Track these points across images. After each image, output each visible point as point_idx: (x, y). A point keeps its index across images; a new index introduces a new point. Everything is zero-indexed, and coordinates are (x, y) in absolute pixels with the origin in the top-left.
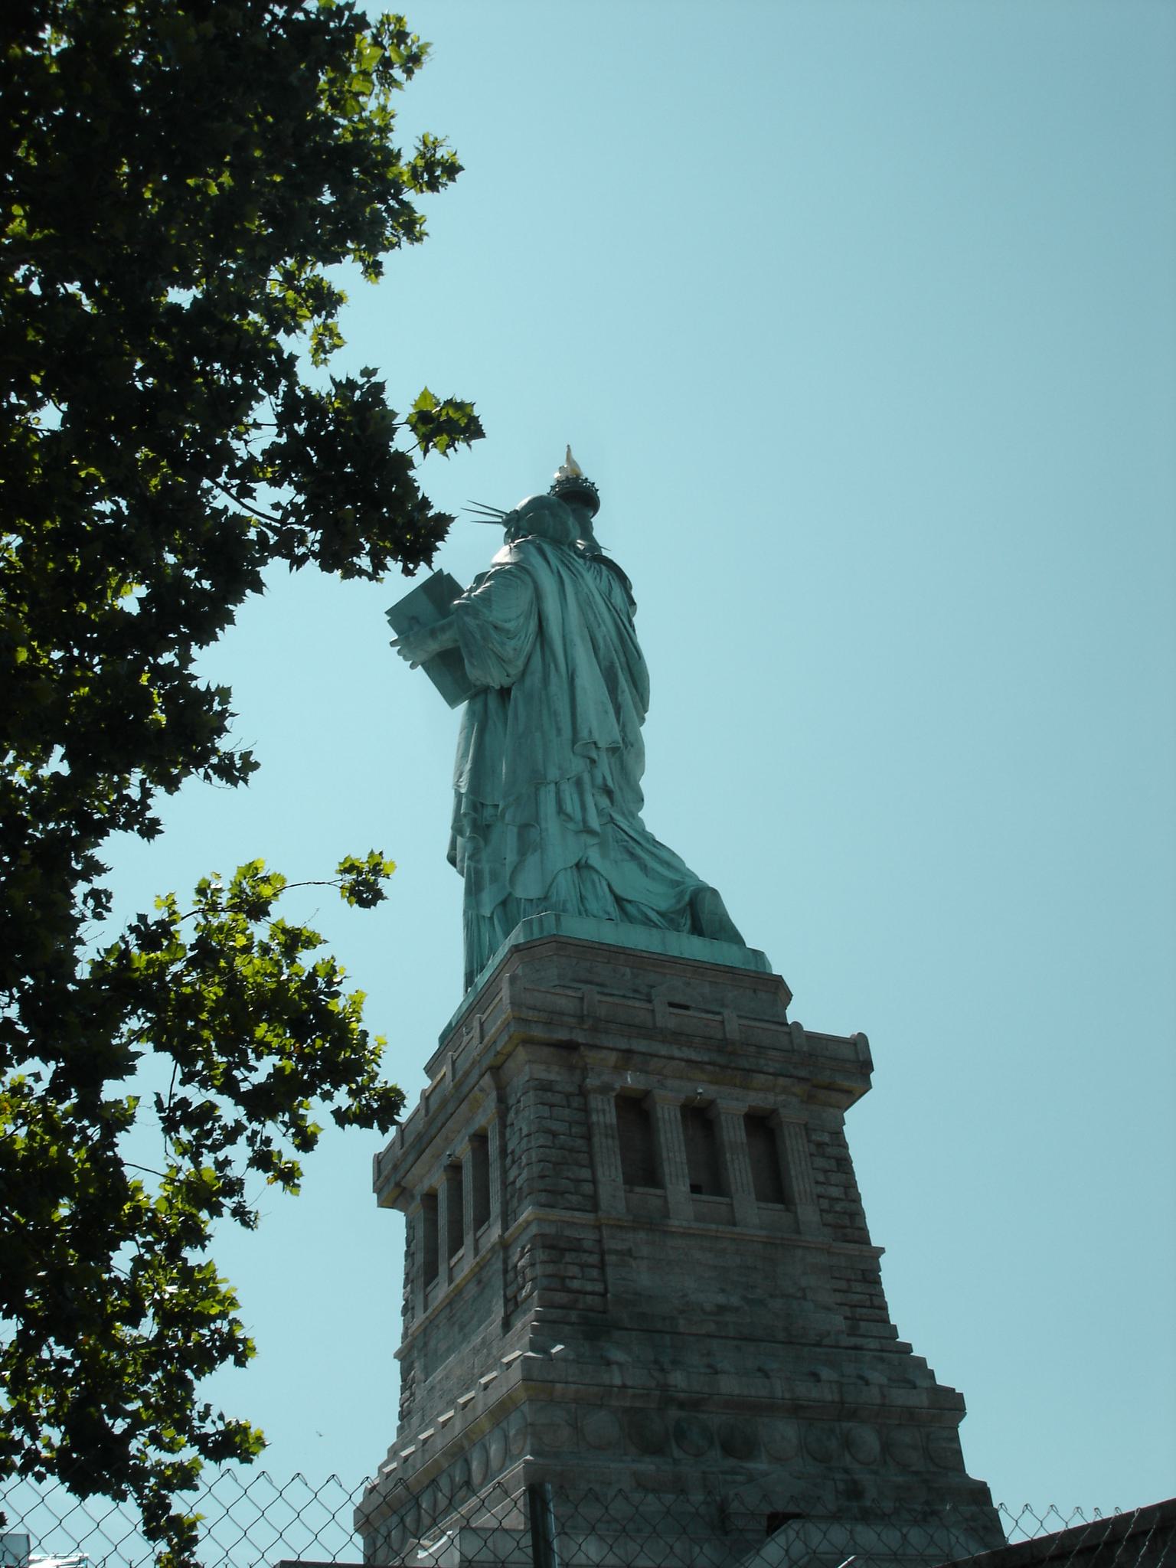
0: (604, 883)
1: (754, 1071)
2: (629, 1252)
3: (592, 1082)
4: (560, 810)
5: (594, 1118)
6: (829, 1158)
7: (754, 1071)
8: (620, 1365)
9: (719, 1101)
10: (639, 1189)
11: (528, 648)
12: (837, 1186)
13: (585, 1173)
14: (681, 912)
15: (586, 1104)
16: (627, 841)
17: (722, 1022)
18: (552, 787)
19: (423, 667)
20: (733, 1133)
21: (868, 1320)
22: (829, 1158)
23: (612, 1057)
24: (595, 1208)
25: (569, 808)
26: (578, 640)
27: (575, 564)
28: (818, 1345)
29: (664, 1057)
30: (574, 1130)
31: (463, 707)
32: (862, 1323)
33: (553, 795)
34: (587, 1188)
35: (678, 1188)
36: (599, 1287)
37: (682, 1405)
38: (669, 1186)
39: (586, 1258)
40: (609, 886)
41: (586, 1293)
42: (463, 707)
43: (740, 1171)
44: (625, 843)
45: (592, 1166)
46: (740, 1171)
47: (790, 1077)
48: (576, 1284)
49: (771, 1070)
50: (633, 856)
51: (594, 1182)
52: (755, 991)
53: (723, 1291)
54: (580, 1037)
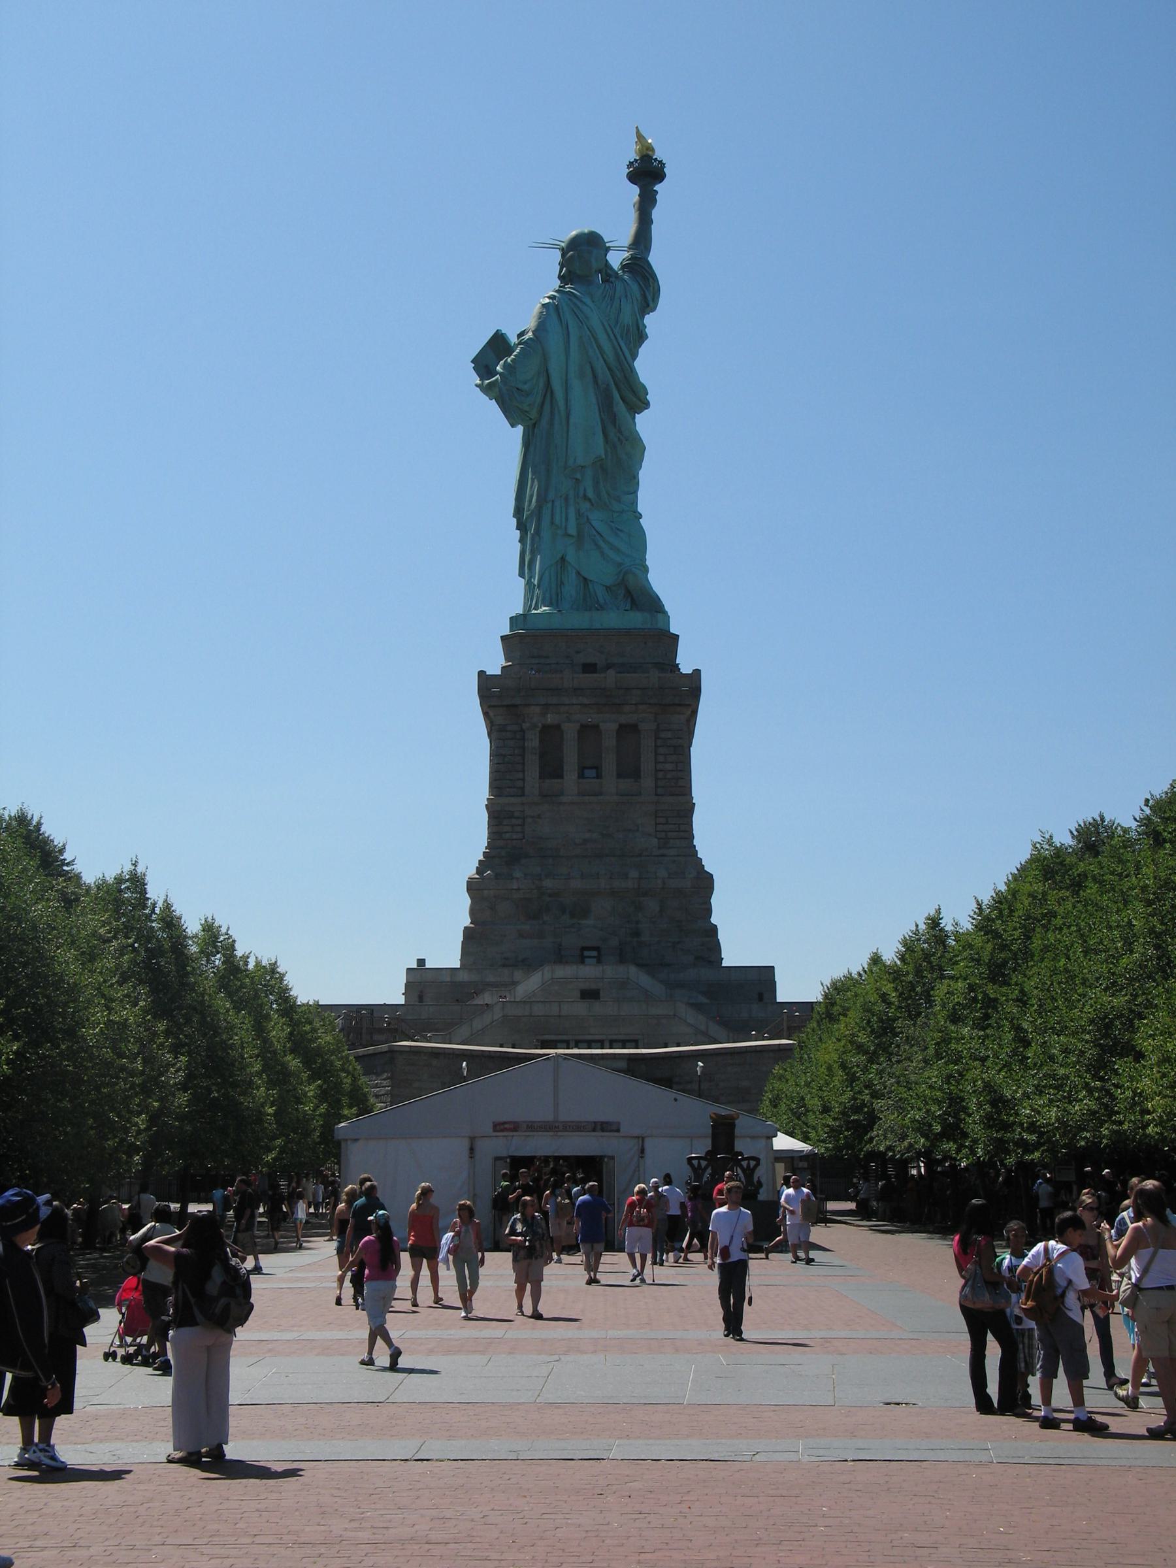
0: (574, 571)
1: (623, 704)
2: (539, 816)
3: (525, 726)
4: (552, 523)
5: (526, 745)
6: (670, 746)
7: (623, 704)
8: (517, 879)
9: (601, 724)
10: (548, 781)
11: (539, 400)
12: (671, 763)
13: (520, 775)
15: (524, 736)
16: (595, 536)
17: (606, 677)
18: (549, 505)
20: (609, 742)
21: (674, 839)
22: (670, 746)
23: (537, 709)
25: (557, 521)
26: (576, 384)
28: (640, 855)
29: (569, 705)
30: (516, 752)
32: (671, 841)
34: (519, 784)
36: (520, 836)
37: (550, 896)
38: (565, 777)
39: (514, 821)
40: (578, 573)
41: (513, 840)
43: (609, 764)
44: (593, 537)
45: (523, 771)
46: (609, 764)
47: (646, 704)
48: (507, 836)
49: (634, 702)
51: (523, 780)
52: (645, 643)
53: (590, 831)
54: (518, 701)
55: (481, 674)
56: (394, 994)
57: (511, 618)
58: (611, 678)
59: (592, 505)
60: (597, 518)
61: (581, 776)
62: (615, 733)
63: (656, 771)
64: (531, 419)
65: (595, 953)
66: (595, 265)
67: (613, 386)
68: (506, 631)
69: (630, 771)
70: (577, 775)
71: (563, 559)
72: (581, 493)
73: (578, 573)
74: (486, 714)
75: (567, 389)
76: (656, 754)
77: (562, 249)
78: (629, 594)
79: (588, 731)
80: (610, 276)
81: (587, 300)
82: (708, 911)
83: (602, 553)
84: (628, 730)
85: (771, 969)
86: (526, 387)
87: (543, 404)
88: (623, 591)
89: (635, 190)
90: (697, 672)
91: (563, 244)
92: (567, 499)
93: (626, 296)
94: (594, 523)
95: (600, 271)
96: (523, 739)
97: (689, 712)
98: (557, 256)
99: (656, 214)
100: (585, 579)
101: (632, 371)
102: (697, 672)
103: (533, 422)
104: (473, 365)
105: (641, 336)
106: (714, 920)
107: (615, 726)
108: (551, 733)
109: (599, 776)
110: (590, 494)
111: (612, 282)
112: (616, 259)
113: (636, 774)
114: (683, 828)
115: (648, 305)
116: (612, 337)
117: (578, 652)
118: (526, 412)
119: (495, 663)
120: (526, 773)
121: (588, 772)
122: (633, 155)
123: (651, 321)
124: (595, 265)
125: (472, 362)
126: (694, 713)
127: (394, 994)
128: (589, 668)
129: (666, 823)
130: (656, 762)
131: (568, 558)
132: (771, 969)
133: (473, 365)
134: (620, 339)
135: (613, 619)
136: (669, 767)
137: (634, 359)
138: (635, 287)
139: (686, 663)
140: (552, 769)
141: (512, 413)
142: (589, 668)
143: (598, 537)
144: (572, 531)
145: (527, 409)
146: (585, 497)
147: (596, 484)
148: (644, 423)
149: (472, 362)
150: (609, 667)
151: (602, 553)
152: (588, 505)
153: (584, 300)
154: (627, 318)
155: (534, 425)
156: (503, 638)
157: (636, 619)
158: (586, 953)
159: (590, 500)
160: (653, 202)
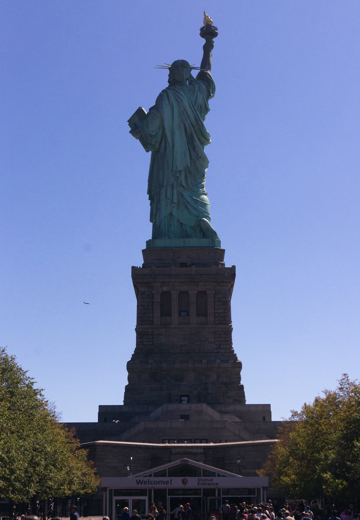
0: (176, 220)
4: (166, 197)
5: (154, 300)
11: (159, 140)
14: (198, 225)
19: (139, 140)
24: (153, 324)
26: (177, 132)
27: (181, 97)
31: (150, 153)
33: (165, 191)
35: (175, 316)
40: (178, 220)
42: (150, 153)
50: (187, 208)
51: (153, 317)
55: (133, 268)
56: (94, 418)
57: (147, 242)
58: (194, 269)
59: (184, 188)
60: (186, 194)
61: (180, 315)
62: (195, 295)
63: (215, 313)
64: (156, 148)
65: (186, 398)
66: (185, 77)
67: (194, 132)
68: (145, 248)
69: (202, 313)
70: (178, 315)
71: (171, 214)
72: (179, 183)
73: (178, 220)
74: (135, 286)
75: (173, 134)
76: (215, 305)
77: (170, 69)
78: (201, 230)
79: (183, 294)
80: (192, 81)
81: (182, 93)
82: (239, 378)
83: (189, 211)
84: (202, 294)
85: (269, 406)
86: (153, 134)
87: (161, 142)
88: (199, 229)
89: (203, 41)
90: (234, 267)
91: (170, 67)
92: (172, 186)
93: (200, 91)
94: (186, 197)
95: (188, 79)
96: (153, 298)
97: (230, 285)
98: (168, 72)
99: (214, 53)
100: (181, 223)
101: (203, 126)
102: (234, 267)
103: (157, 150)
104: (128, 123)
105: (207, 110)
106: (242, 382)
107: (196, 292)
108: (166, 295)
109: (188, 315)
110: (184, 184)
111: (193, 84)
112: (195, 73)
113: (206, 315)
114: (227, 339)
115: (210, 95)
116: (193, 109)
117: (178, 258)
118: (154, 145)
119: (139, 262)
120: (154, 314)
121: (183, 314)
122: (202, 25)
123: (211, 102)
124: (185, 77)
125: (128, 121)
126: (232, 286)
127: (94, 418)
128: (183, 265)
129: (220, 337)
130: (215, 309)
131: (174, 214)
132: (269, 406)
133: (128, 123)
134: (197, 111)
135: (194, 242)
136: (220, 311)
137: (204, 120)
138: (204, 87)
139: (228, 262)
140: (166, 313)
141: (146, 145)
142: (183, 265)
143: (187, 203)
144: (175, 201)
145: (154, 143)
146: (181, 185)
147: (186, 178)
148: (207, 150)
149: (128, 121)
150: (193, 264)
151: (189, 211)
152: (182, 189)
153: (180, 93)
154: (200, 100)
155: (157, 151)
156: (143, 251)
157: (204, 242)
158: (183, 398)
159: (183, 186)
160: (212, 46)
